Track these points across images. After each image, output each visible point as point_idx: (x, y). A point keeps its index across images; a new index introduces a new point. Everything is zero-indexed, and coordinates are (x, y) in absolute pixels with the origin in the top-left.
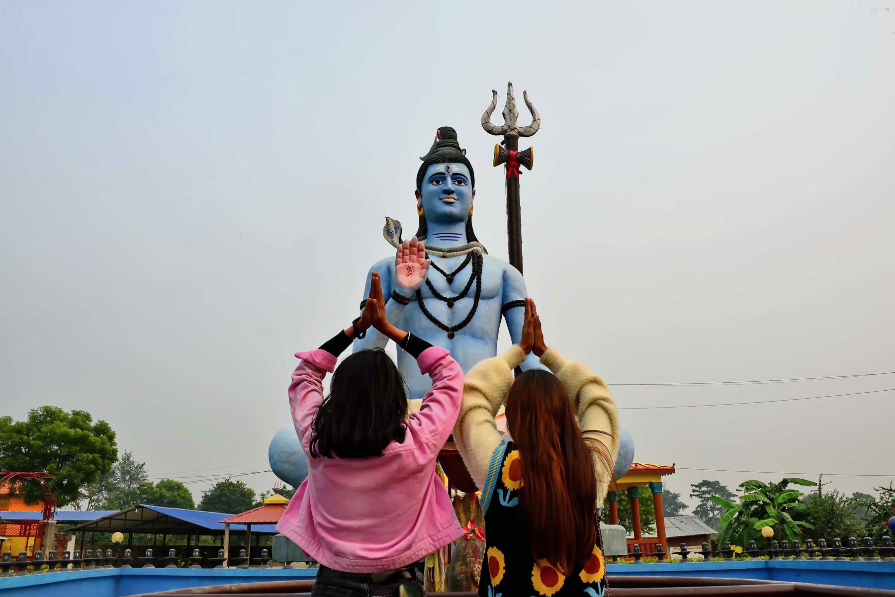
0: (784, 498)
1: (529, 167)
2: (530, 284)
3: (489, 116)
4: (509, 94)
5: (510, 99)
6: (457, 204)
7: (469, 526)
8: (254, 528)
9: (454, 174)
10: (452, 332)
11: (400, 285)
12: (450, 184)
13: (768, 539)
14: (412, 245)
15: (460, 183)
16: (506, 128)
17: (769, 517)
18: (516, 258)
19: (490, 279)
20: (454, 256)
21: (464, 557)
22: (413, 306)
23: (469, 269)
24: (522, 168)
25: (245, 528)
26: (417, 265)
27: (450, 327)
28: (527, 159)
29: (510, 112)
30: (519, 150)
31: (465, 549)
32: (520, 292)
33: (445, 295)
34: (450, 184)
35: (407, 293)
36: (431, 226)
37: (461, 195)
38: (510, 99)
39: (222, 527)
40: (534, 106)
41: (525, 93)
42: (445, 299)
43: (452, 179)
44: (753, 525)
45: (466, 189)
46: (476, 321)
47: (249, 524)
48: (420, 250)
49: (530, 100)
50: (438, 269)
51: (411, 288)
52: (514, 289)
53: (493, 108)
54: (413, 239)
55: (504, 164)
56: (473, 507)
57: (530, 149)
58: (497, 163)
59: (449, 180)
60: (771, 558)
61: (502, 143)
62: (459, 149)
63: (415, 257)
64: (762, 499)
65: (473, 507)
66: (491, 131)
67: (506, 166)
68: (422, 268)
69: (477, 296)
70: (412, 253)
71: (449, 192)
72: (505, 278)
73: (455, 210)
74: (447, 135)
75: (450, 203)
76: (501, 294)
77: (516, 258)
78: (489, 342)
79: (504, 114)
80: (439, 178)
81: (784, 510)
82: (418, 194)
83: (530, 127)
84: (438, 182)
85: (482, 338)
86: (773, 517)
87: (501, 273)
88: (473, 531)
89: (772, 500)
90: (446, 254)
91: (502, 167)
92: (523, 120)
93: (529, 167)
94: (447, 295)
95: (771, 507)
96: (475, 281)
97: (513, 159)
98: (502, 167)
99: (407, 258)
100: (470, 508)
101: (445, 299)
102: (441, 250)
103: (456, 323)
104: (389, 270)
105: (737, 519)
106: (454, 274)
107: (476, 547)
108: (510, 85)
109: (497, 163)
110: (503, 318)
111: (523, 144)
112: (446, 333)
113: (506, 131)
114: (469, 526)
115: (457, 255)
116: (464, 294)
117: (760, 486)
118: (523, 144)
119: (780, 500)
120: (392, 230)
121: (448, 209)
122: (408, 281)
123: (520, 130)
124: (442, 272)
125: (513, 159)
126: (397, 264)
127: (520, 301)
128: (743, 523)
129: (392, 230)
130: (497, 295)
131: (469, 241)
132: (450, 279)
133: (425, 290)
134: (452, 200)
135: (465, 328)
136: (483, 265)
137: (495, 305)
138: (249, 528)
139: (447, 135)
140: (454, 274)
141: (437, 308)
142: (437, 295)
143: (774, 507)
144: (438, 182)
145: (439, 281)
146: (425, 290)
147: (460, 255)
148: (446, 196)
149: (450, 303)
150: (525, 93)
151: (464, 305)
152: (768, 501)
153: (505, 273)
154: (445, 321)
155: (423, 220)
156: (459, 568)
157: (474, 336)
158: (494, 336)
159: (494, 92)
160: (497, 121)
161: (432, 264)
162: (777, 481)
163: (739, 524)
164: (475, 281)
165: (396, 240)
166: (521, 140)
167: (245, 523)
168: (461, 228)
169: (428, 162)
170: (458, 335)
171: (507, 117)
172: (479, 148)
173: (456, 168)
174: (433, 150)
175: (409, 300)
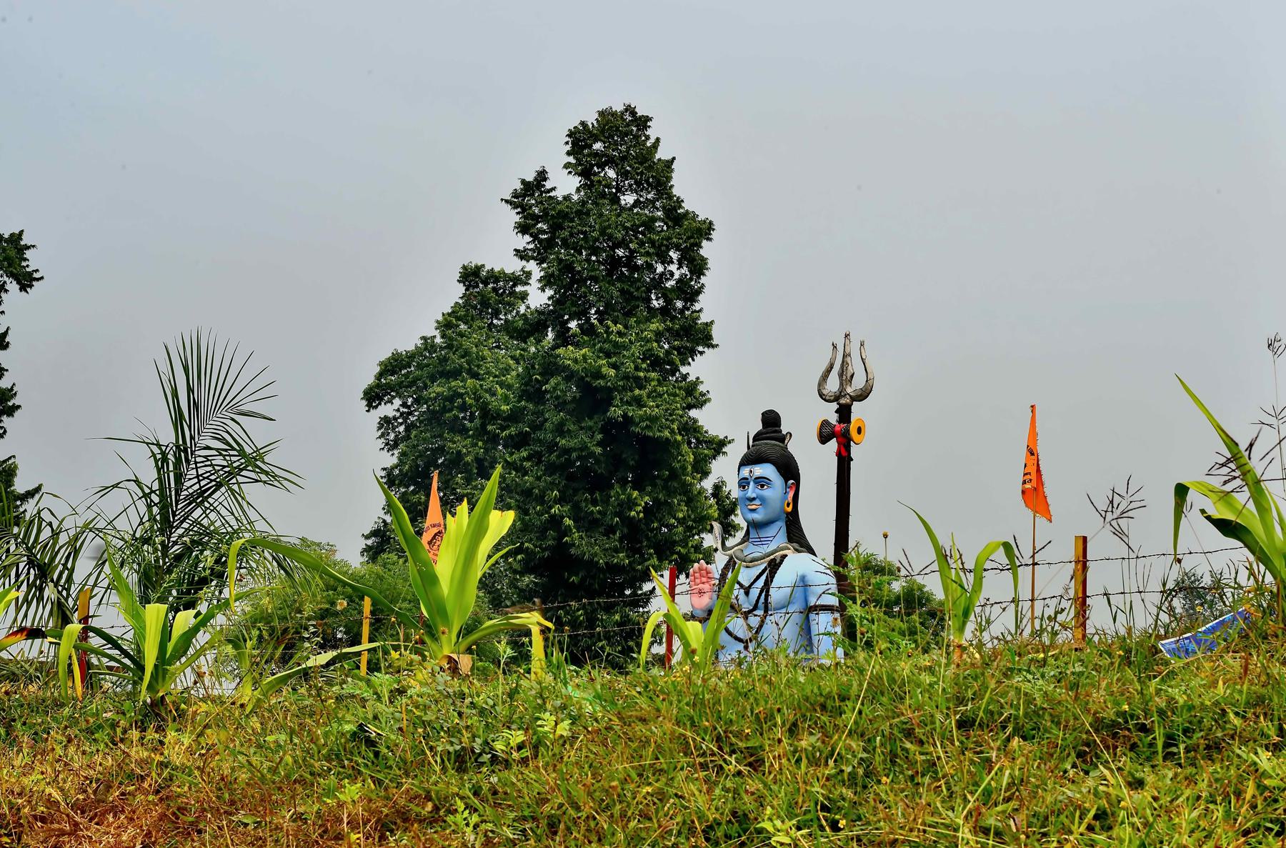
15: (762, 486)
37: (763, 500)
63: (704, 580)
70: (701, 576)
71: (754, 499)
74: (771, 420)
91: (833, 444)
106: (750, 586)
125: (839, 434)
139: (771, 420)
140: (750, 586)
149: (746, 615)
154: (740, 635)
159: (835, 347)
160: (833, 385)
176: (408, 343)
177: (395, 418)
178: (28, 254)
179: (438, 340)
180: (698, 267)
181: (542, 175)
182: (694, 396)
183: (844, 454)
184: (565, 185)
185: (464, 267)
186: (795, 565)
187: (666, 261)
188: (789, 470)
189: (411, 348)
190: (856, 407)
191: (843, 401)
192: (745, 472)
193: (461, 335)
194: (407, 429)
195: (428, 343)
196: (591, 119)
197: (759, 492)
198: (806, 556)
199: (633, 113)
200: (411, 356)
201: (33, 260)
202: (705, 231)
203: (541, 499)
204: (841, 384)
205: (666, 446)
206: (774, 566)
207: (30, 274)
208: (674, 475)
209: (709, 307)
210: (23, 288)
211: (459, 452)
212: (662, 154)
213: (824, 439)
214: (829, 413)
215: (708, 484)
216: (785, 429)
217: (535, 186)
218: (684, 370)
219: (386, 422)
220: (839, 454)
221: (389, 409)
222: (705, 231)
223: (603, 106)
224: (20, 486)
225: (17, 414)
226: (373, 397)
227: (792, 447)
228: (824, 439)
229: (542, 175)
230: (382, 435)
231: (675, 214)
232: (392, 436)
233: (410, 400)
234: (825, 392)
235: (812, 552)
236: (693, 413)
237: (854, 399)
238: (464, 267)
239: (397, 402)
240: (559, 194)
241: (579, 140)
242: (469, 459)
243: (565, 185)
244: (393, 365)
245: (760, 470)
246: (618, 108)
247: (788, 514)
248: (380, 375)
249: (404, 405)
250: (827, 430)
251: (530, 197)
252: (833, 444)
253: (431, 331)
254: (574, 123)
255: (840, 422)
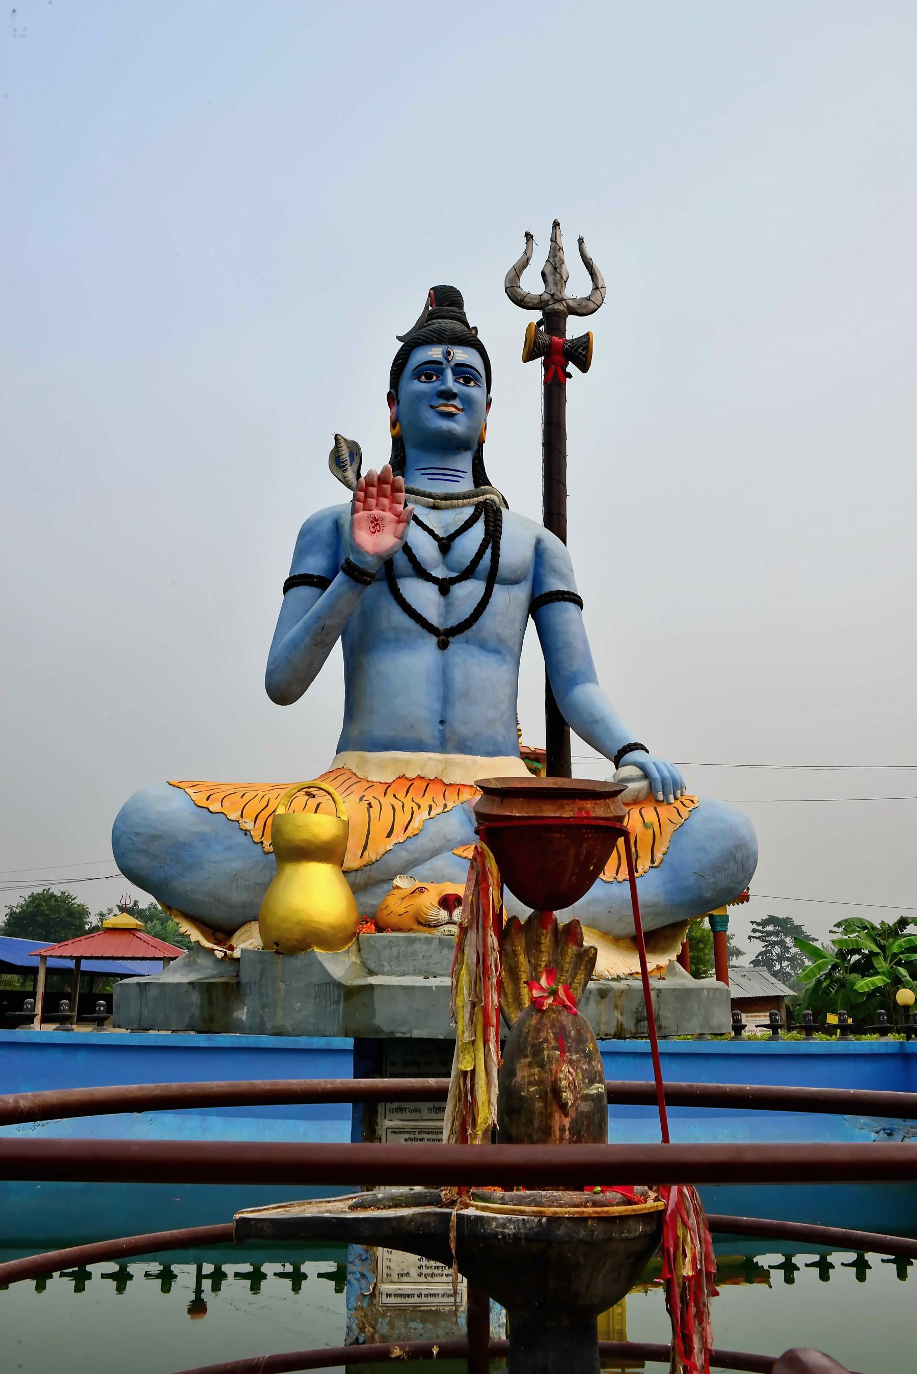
0: (900, 946)
1: (584, 367)
2: (582, 561)
3: (518, 276)
4: (554, 240)
5: (556, 249)
6: (461, 417)
7: (543, 982)
8: (86, 966)
9: (457, 365)
10: (445, 637)
11: (356, 549)
12: (450, 382)
13: (906, 1008)
14: (382, 480)
15: (467, 382)
16: (546, 297)
17: (877, 973)
18: (555, 517)
19: (515, 548)
20: (453, 507)
21: (537, 1050)
22: (377, 589)
23: (478, 531)
24: (571, 368)
25: (71, 964)
26: (388, 515)
27: (441, 628)
28: (581, 352)
29: (554, 271)
30: (569, 336)
31: (538, 1031)
32: (564, 577)
33: (434, 574)
34: (450, 382)
35: (371, 565)
36: (411, 453)
37: (468, 403)
38: (556, 249)
39: (35, 962)
40: (597, 263)
41: (581, 241)
42: (435, 580)
43: (454, 373)
44: (853, 984)
45: (476, 392)
46: (489, 622)
47: (78, 959)
48: (396, 489)
49: (590, 253)
50: (425, 528)
51: (378, 556)
52: (555, 571)
53: (525, 263)
54: (385, 470)
55: (540, 360)
56: (546, 941)
57: (588, 335)
58: (529, 356)
60: (909, 1038)
61: (540, 324)
62: (467, 325)
63: (386, 501)
64: (869, 947)
65: (546, 941)
66: (521, 301)
67: (545, 364)
68: (399, 522)
69: (492, 578)
70: (381, 494)
71: (448, 395)
72: (539, 550)
73: (458, 426)
74: (445, 300)
75: (450, 416)
76: (530, 577)
77: (555, 517)
78: (508, 658)
79: (543, 274)
80: (431, 371)
81: (899, 963)
82: (392, 399)
83: (588, 299)
84: (429, 377)
85: (497, 651)
86: (883, 974)
87: (533, 542)
88: (554, 993)
89: (883, 948)
90: (438, 503)
91: (537, 366)
92: (577, 286)
93: (584, 367)
94: (439, 573)
95: (881, 958)
96: (489, 552)
97: (558, 353)
98: (537, 366)
99: (373, 502)
100: (539, 943)
101: (435, 580)
102: (430, 496)
103: (453, 622)
104: (337, 526)
105: (829, 975)
107: (563, 1027)
108: (556, 224)
109: (529, 356)
110: (531, 622)
111: (574, 327)
112: (434, 640)
113: (547, 303)
114: (543, 982)
115: (459, 507)
116: (468, 573)
117: (865, 928)
118: (574, 327)
119: (895, 949)
120: (344, 456)
121: (445, 424)
122: (374, 542)
123: (571, 303)
124: (431, 532)
125: (558, 353)
126: (354, 511)
127: (563, 592)
128: (837, 981)
129: (344, 456)
130: (525, 578)
131: (477, 484)
132: (445, 545)
133: (401, 561)
134: (452, 410)
135: (468, 633)
136: (504, 525)
137: (520, 594)
138: (78, 964)
139: (445, 300)
141: (422, 595)
142: (421, 573)
143: (885, 959)
144: (429, 377)
145: (425, 548)
146: (401, 561)
147: (464, 506)
148: (442, 401)
149: (444, 586)
150: (581, 241)
151: (469, 592)
152: (877, 950)
153: (539, 542)
154: (432, 615)
155: (398, 444)
156: (523, 1073)
157: (483, 646)
158: (516, 649)
159: (529, 237)
161: (415, 518)
162: (891, 921)
163: (832, 982)
164: (489, 552)
165: (350, 475)
166: (571, 320)
167: (71, 958)
168: (464, 462)
169: (411, 343)
170: (456, 645)
171: (550, 279)
172: (501, 328)
173: (461, 355)
174: (420, 324)
175: (372, 576)
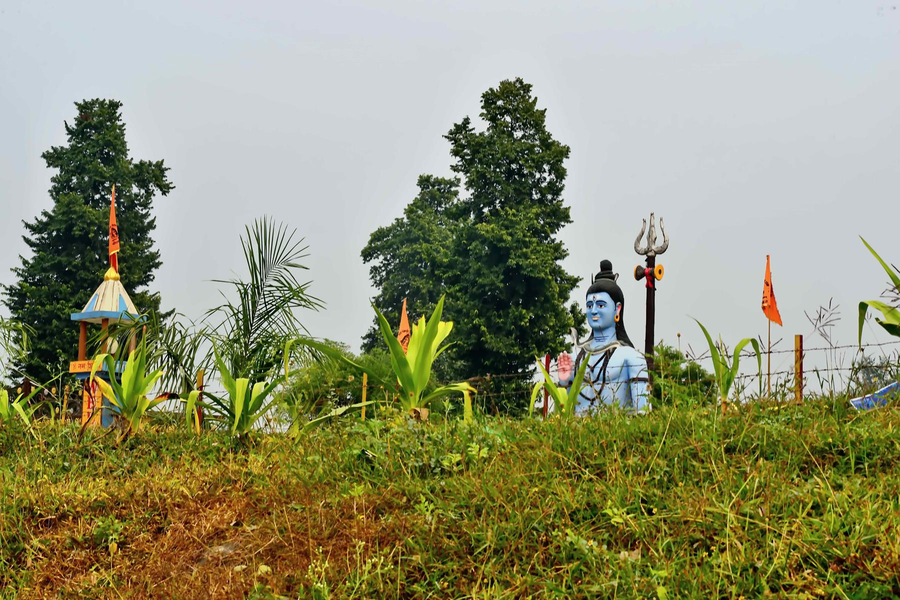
5: (651, 226)
37: (602, 314)
59: (595, 305)
74: (606, 266)
91: (644, 280)
125: (648, 274)
139: (606, 266)
154: (589, 396)
159: (645, 221)
160: (644, 245)
166: (658, 257)
176: (388, 222)
177: (380, 267)
178: (166, 173)
179: (406, 220)
180: (561, 174)
181: (467, 121)
182: (558, 252)
183: (651, 286)
184: (480, 126)
185: (421, 177)
186: (621, 353)
187: (541, 171)
188: (617, 296)
189: (389, 225)
190: (659, 260)
191: (650, 254)
192: (591, 297)
193: (419, 217)
194: (387, 274)
195: (399, 223)
196: (496, 87)
197: (599, 309)
198: (628, 348)
199: (521, 82)
200: (389, 230)
201: (169, 177)
202: (564, 152)
203: (467, 315)
204: (649, 244)
205: (542, 281)
206: (608, 355)
207: (168, 185)
208: (547, 300)
209: (567, 198)
210: (164, 193)
211: (418, 287)
212: (539, 107)
213: (638, 277)
214: (642, 262)
215: (568, 305)
216: (614, 271)
217: (462, 127)
218: (553, 236)
219: (375, 270)
220: (647, 286)
221: (376, 262)
222: (564, 152)
223: (503, 79)
224: (162, 309)
225: (161, 267)
226: (367, 255)
227: (619, 282)
228: (638, 277)
229: (467, 121)
230: (373, 277)
231: (547, 143)
232: (378, 278)
233: (389, 257)
234: (639, 249)
235: (631, 345)
236: (558, 262)
237: (656, 253)
238: (421, 177)
239: (381, 258)
240: (477, 132)
241: (489, 99)
242: (424, 291)
243: (480, 126)
244: (379, 236)
245: (600, 296)
246: (512, 79)
247: (617, 323)
248: (371, 242)
249: (385, 259)
250: (640, 272)
251: (460, 134)
252: (644, 280)
253: (402, 215)
254: (486, 89)
255: (648, 266)
